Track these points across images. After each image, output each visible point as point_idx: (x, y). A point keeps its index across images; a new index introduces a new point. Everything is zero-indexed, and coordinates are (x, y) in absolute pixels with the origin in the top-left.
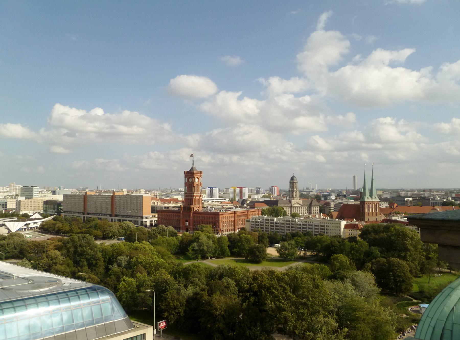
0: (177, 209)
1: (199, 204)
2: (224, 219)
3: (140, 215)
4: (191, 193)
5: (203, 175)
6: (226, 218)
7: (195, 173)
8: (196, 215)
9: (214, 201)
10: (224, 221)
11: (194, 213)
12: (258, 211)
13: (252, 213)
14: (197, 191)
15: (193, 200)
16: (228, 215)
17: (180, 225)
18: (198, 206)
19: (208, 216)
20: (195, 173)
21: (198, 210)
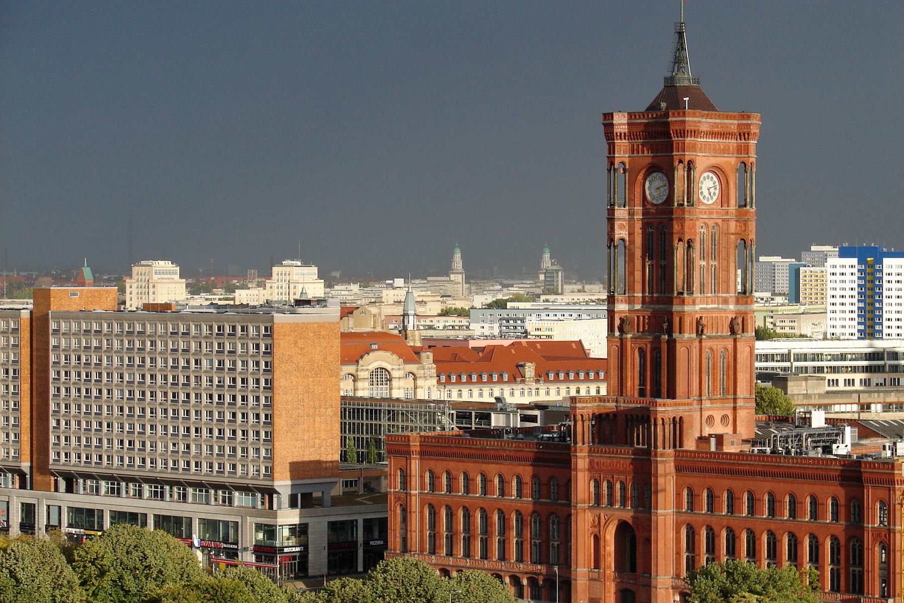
3: (251, 473)
21: (720, 439)
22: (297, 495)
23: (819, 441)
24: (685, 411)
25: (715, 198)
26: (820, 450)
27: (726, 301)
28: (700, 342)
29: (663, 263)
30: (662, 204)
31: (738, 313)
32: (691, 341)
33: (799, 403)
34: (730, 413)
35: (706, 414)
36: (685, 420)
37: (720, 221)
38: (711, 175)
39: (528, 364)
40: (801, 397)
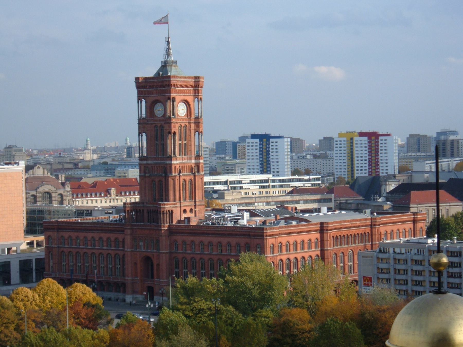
0: (114, 217)
1: (193, 197)
2: (280, 250)
4: (162, 159)
5: (204, 92)
6: (288, 250)
7: (175, 86)
8: (179, 239)
9: (268, 187)
10: (284, 258)
11: (172, 231)
12: (415, 221)
13: (389, 228)
14: (185, 150)
15: (171, 182)
16: (299, 238)
17: (124, 275)
18: (188, 204)
19: (224, 240)
20: (175, 86)
21: (189, 219)
22: (5, 249)
23: (232, 219)
24: (173, 207)
25: (185, 114)
26: (233, 223)
27: (190, 159)
28: (180, 177)
29: (162, 142)
30: (162, 117)
31: (195, 163)
32: (175, 176)
33: (230, 202)
34: (193, 208)
35: (183, 209)
36: (174, 211)
37: (187, 124)
38: (183, 103)
39: (113, 189)
40: (230, 200)
